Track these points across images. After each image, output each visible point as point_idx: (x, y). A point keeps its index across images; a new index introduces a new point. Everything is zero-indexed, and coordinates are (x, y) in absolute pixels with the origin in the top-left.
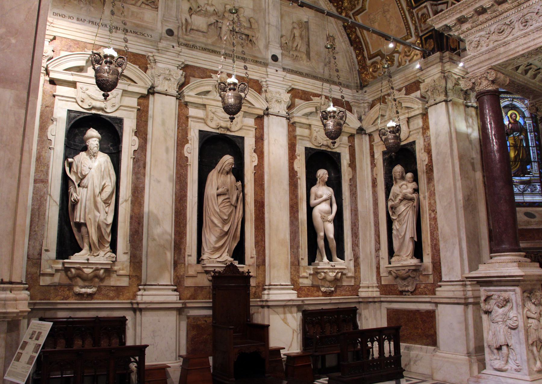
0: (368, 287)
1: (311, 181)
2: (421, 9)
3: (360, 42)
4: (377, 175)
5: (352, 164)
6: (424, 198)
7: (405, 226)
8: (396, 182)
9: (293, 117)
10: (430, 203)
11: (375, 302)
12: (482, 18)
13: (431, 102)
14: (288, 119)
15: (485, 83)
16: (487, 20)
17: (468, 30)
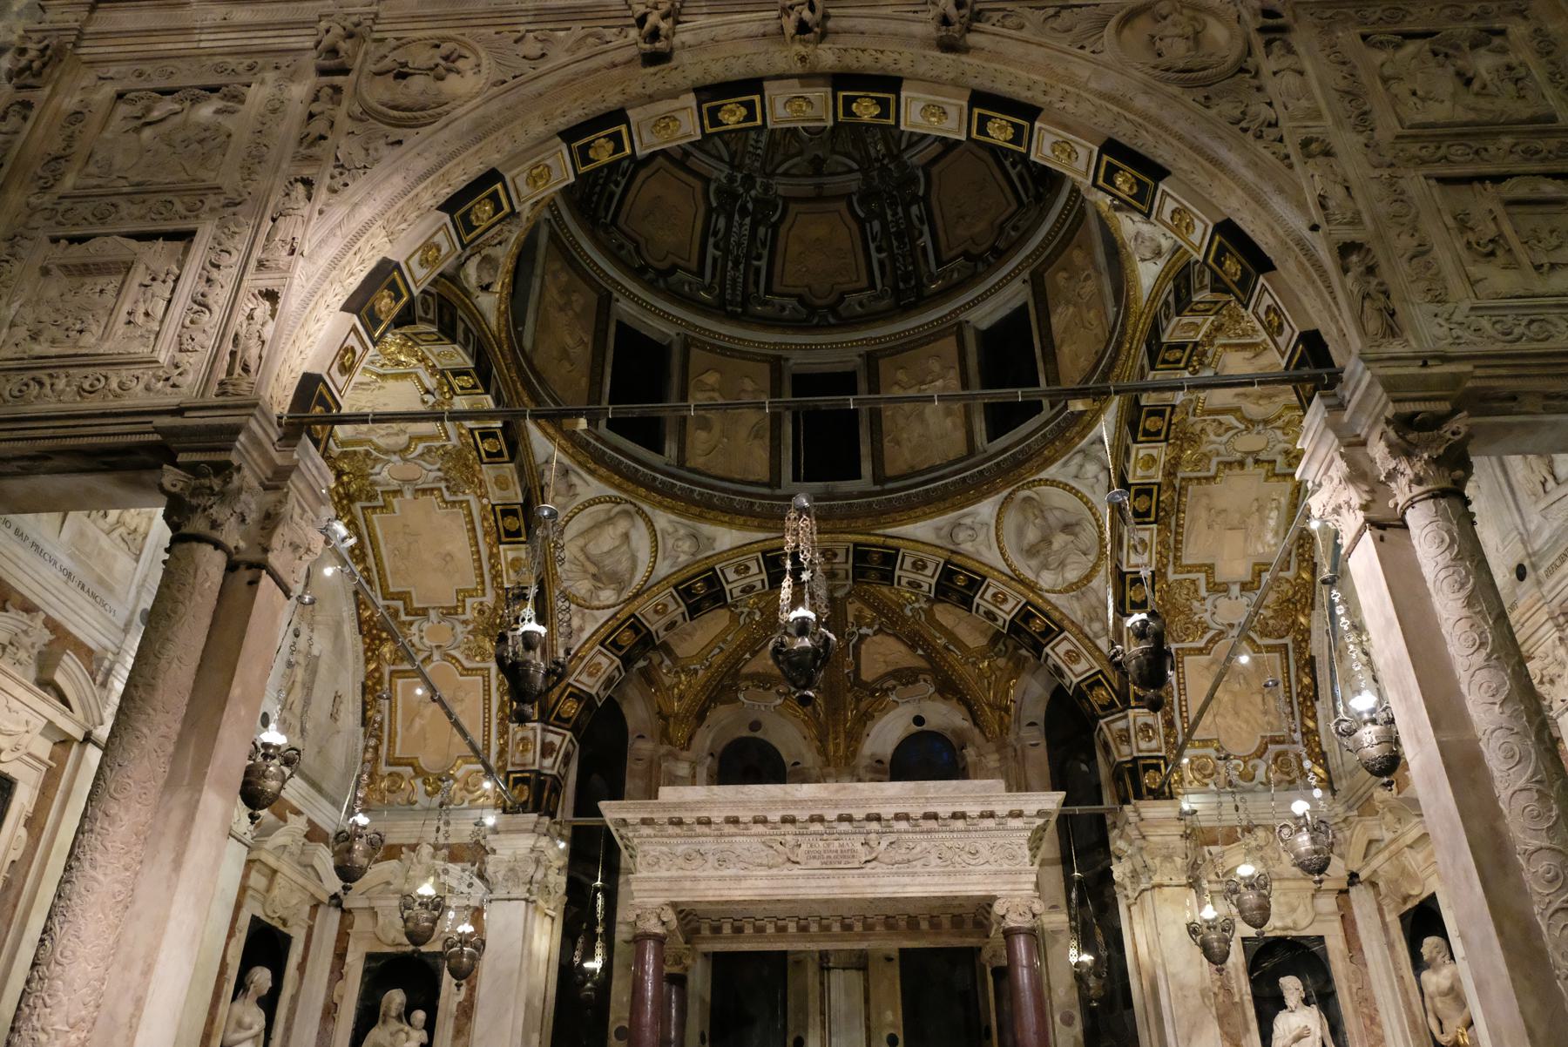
1: (241, 986)
4: (341, 997)
8: (384, 1022)
9: (260, 849)
12: (671, 830)
13: (500, 892)
15: (654, 920)
16: (678, 836)
17: (649, 836)
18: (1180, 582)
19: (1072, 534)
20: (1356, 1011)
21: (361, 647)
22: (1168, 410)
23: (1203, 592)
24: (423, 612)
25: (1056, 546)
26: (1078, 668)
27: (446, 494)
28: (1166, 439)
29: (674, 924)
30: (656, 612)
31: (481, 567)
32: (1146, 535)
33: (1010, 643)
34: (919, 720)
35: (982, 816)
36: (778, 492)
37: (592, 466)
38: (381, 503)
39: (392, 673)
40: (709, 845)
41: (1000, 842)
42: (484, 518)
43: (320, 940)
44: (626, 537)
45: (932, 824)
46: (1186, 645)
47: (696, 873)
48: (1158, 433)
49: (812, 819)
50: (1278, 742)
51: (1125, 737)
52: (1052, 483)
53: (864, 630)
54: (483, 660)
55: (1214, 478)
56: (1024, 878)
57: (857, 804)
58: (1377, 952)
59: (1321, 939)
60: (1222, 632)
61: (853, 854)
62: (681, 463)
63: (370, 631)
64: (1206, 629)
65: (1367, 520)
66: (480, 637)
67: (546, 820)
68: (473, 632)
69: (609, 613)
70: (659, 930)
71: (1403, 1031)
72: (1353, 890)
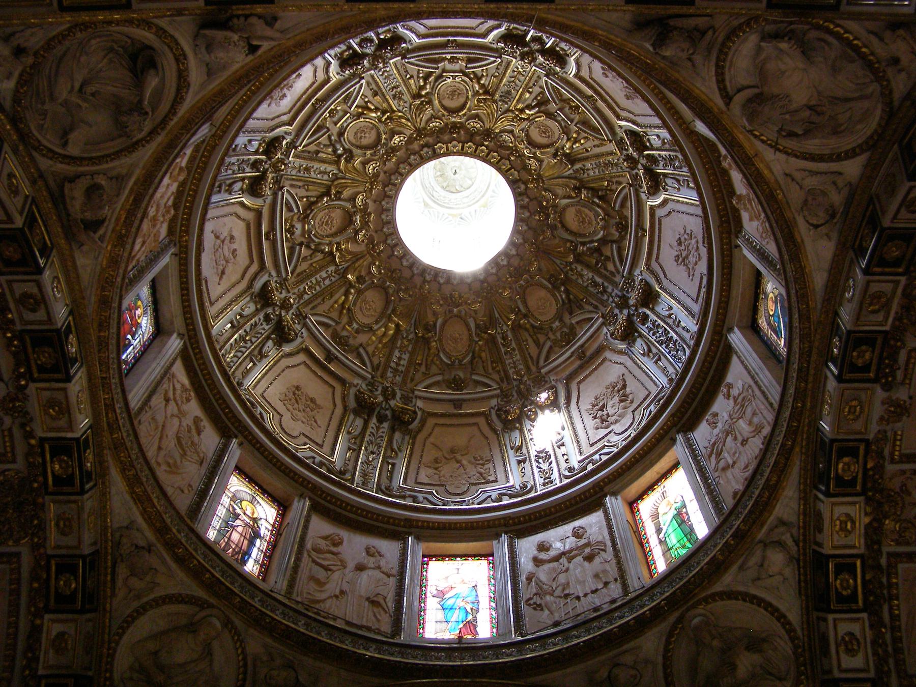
22: (862, 448)
32: (856, 628)
52: (730, 595)
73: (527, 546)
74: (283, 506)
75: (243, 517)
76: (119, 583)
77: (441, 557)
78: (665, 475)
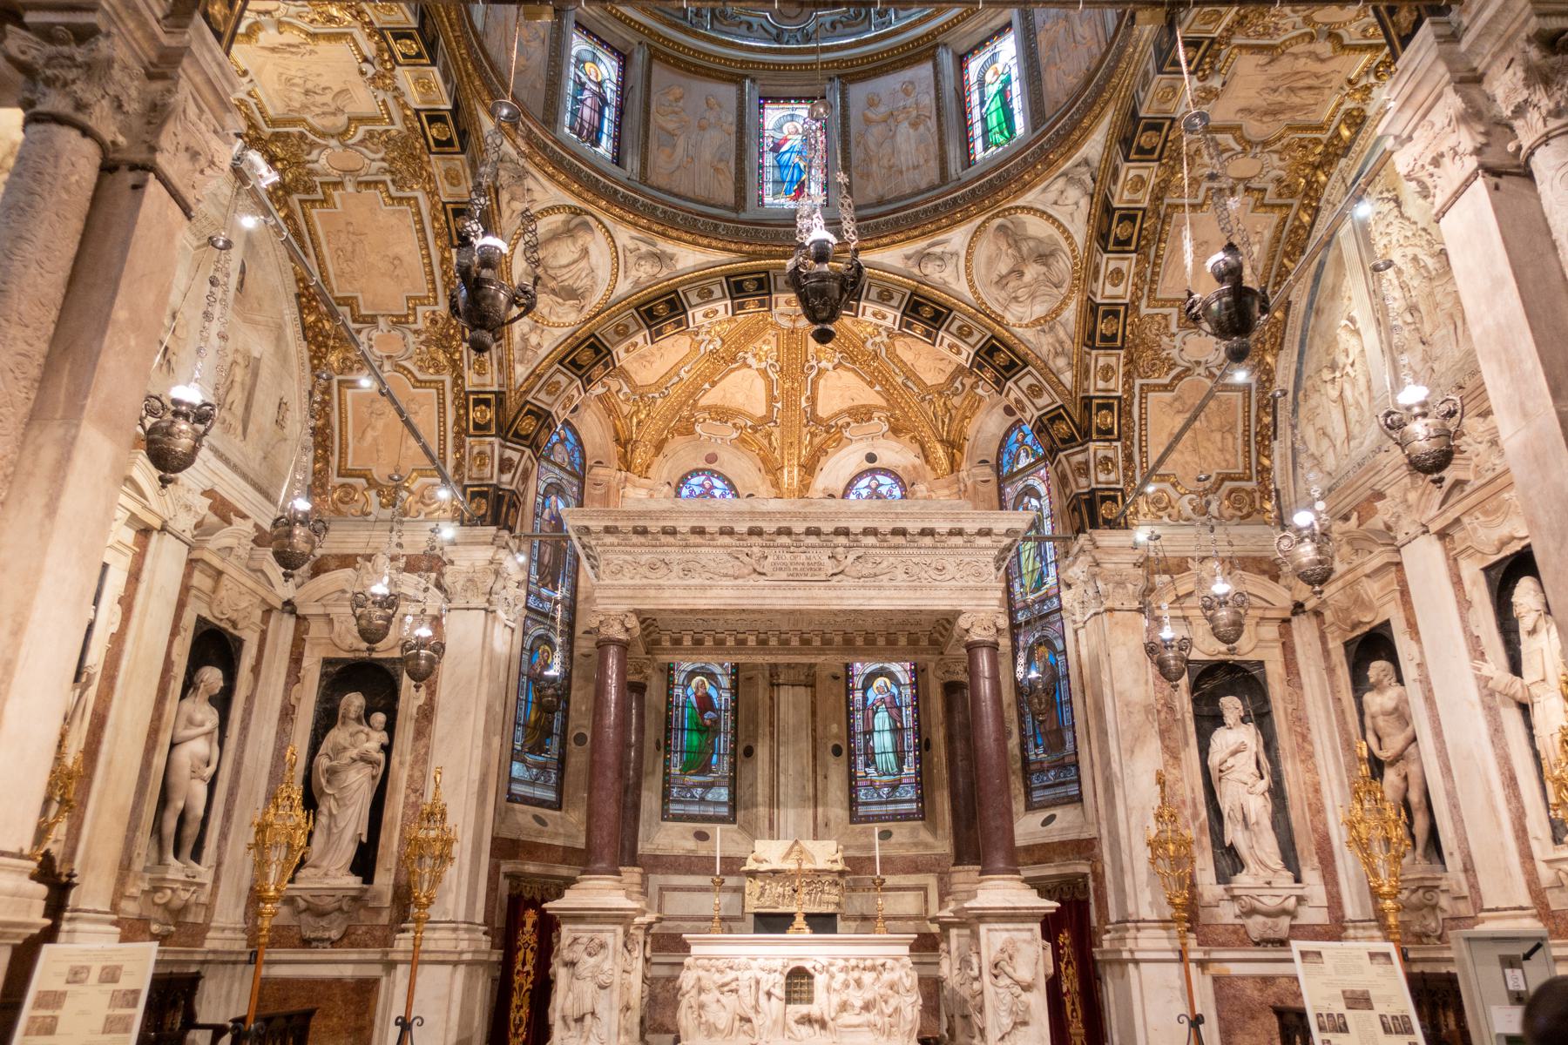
0: (223, 929)
1: (189, 686)
2: (481, 443)
3: (330, 437)
4: (299, 700)
5: (256, 670)
6: (401, 763)
7: (350, 811)
9: (203, 548)
10: (411, 776)
11: (235, 963)
12: (635, 539)
14: (191, 548)
15: (617, 627)
16: (642, 545)
17: (612, 545)
18: (1152, 316)
19: (1045, 264)
20: (1290, 729)
21: (306, 354)
22: (1168, 123)
23: (1174, 328)
24: (372, 320)
25: (1028, 277)
26: (1040, 402)
27: (392, 189)
28: (1159, 159)
29: (637, 631)
30: (617, 333)
31: (432, 273)
33: (968, 381)
34: (871, 458)
35: (951, 533)
36: (743, 216)
37: (550, 170)
38: (319, 195)
39: (340, 382)
40: (674, 555)
41: (967, 559)
42: (435, 218)
43: (275, 645)
44: (585, 252)
45: (900, 540)
46: (1151, 381)
47: (660, 582)
48: (1152, 151)
49: (780, 532)
50: (1233, 479)
51: (1083, 470)
53: (824, 364)
54: (437, 372)
55: (1201, 206)
56: (989, 594)
57: (827, 517)
58: (1314, 677)
59: (1261, 664)
60: (1188, 369)
61: (819, 567)
62: (644, 179)
63: (315, 337)
64: (1175, 364)
65: (1481, 166)
66: (433, 348)
67: (505, 533)
68: (426, 343)
69: (567, 331)
70: (623, 636)
71: (1334, 749)
72: (1295, 620)
73: (858, 92)
74: (624, 59)
75: (590, 85)
76: (504, 205)
77: (776, 99)
78: (1000, 32)
